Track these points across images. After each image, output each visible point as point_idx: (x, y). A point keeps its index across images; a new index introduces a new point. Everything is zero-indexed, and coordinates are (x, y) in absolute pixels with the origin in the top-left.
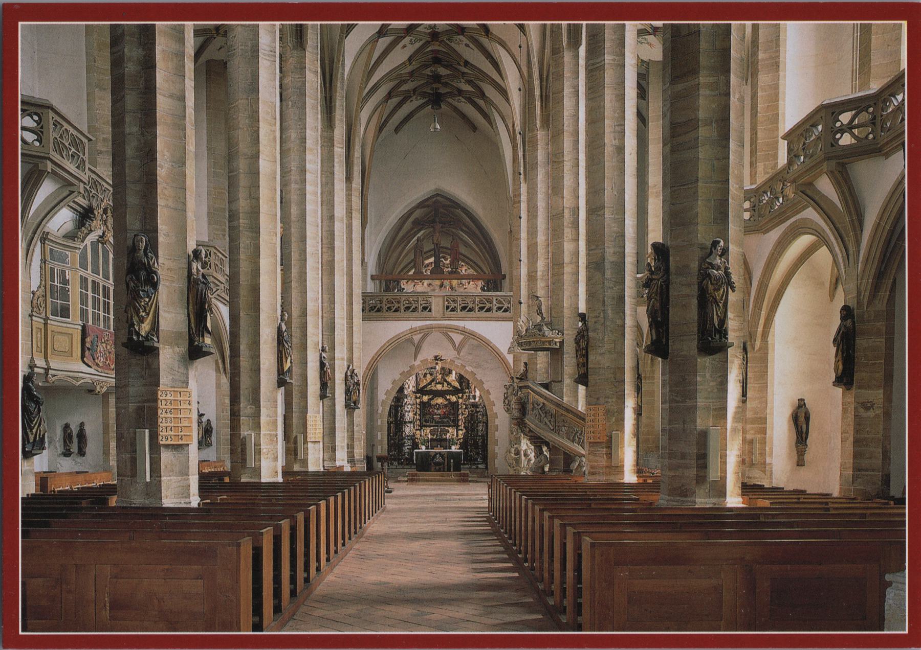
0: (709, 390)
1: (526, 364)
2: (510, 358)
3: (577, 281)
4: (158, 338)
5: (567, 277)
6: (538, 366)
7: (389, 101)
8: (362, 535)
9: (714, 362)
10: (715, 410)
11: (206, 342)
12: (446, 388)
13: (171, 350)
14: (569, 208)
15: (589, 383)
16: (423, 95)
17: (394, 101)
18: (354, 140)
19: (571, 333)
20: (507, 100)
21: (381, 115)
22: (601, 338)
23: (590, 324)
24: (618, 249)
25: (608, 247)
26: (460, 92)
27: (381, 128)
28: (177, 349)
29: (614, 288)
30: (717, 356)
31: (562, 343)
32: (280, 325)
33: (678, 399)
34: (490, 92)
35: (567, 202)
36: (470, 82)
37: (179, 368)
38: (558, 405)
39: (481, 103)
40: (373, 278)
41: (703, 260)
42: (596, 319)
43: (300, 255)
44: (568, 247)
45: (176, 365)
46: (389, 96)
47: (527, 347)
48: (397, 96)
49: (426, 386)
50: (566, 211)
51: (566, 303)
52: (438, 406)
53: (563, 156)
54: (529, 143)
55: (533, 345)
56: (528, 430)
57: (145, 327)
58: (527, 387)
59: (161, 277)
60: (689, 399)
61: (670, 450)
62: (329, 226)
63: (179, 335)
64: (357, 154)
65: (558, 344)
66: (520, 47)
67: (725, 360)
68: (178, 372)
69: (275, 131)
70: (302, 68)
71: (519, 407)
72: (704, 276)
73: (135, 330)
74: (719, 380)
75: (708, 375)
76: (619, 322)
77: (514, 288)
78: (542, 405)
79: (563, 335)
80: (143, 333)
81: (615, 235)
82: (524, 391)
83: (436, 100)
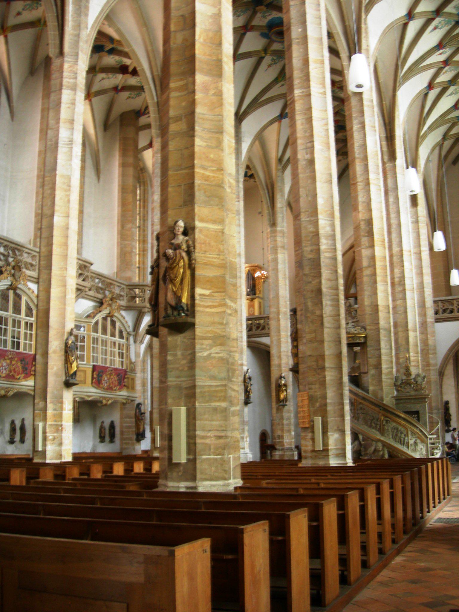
0: (180, 368)
9: (185, 340)
10: (186, 388)
14: (365, 220)
15: (300, 372)
19: (372, 327)
29: (313, 282)
30: (187, 334)
32: (67, 339)
50: (362, 223)
67: (193, 337)
74: (189, 357)
75: (179, 353)
76: (318, 313)
81: (311, 235)
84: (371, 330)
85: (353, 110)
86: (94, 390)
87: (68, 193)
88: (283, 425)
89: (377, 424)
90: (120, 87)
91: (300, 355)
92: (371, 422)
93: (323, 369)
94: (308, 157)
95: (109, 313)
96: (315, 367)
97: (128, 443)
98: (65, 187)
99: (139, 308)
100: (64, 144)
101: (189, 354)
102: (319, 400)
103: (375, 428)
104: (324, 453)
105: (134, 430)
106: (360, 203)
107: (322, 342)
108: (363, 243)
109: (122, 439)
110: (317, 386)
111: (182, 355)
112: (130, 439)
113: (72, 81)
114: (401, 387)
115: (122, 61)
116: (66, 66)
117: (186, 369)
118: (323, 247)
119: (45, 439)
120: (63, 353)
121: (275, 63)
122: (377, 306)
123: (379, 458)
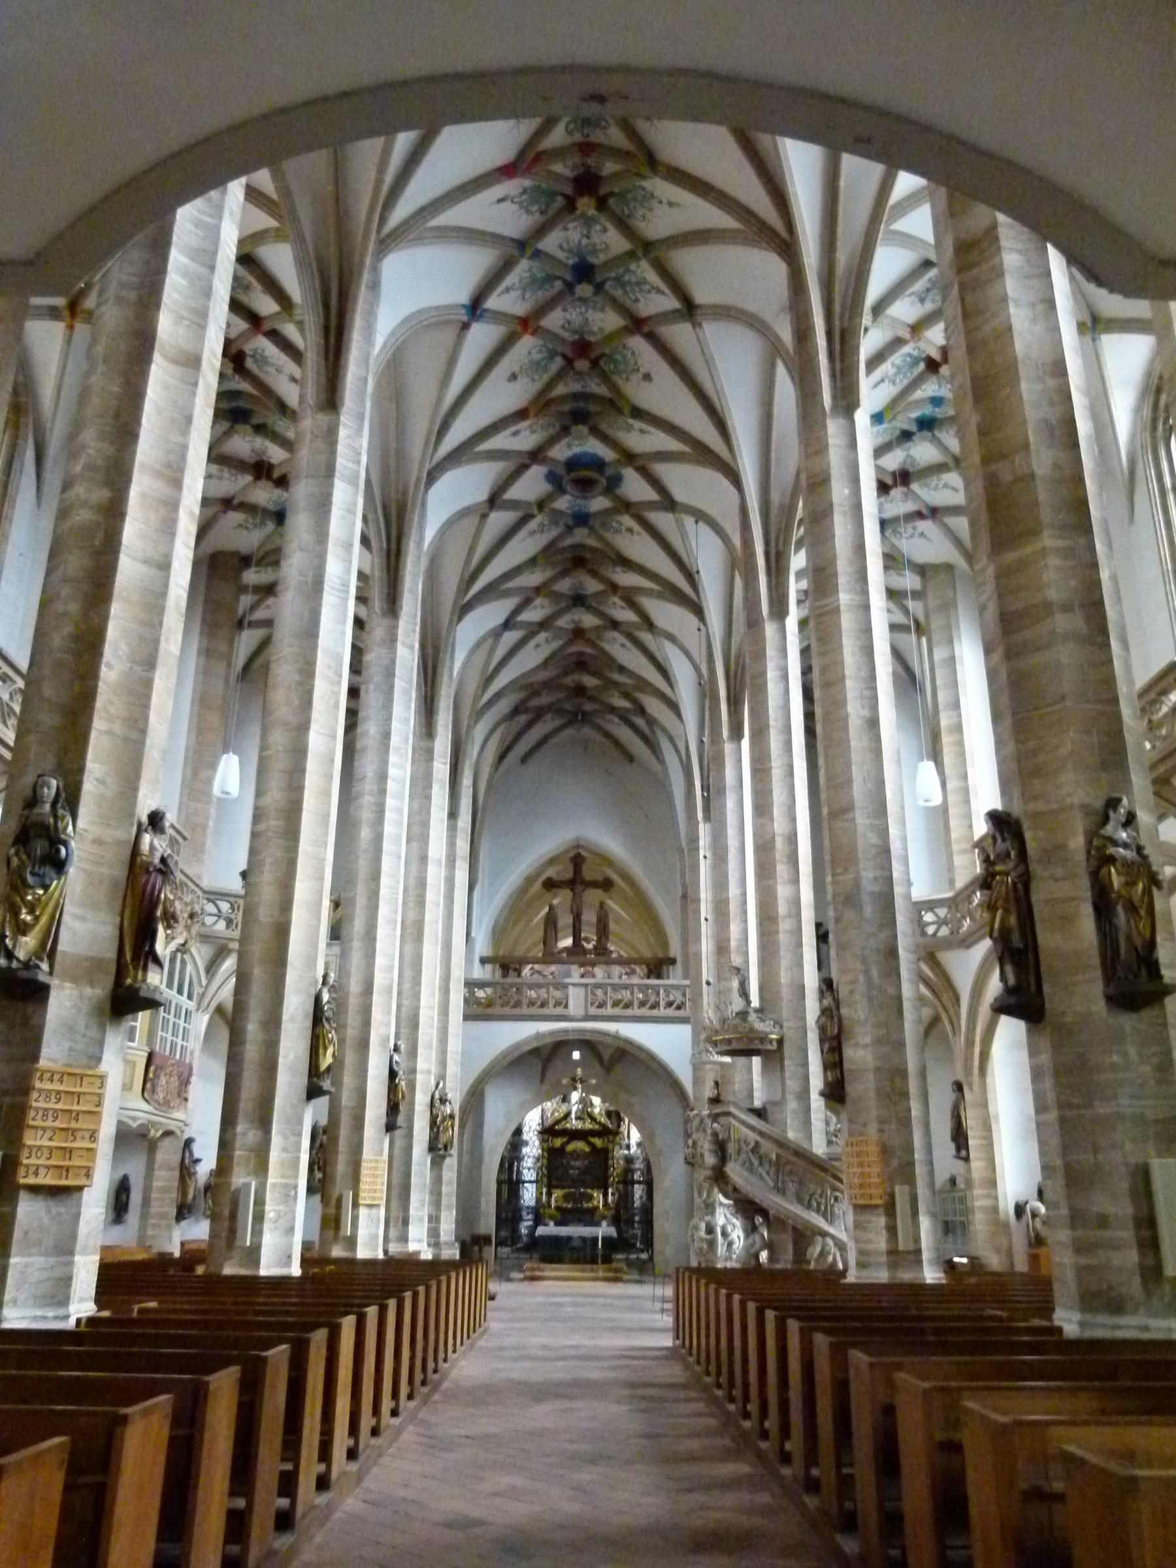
1: (717, 1084)
2: (685, 1076)
3: (800, 945)
4: (51, 967)
5: (783, 938)
6: (737, 1087)
7: (516, 719)
8: (436, 1386)
10: (1157, 1121)
11: (149, 980)
12: (589, 1125)
13: (75, 993)
15: (848, 1098)
16: (560, 712)
17: (523, 719)
18: (464, 762)
20: (678, 714)
21: (502, 740)
22: (862, 1017)
23: (843, 991)
24: (879, 873)
25: (865, 869)
26: (612, 709)
27: (502, 757)
28: (88, 991)
30: (1147, 1014)
31: (780, 1042)
33: (1076, 1101)
34: (654, 706)
35: (779, 825)
36: (626, 695)
37: (87, 1026)
38: (782, 1144)
39: (640, 722)
40: (484, 961)
41: (1092, 834)
42: (851, 987)
43: (370, 899)
44: (783, 892)
45: (81, 1027)
46: (516, 711)
47: (726, 1048)
48: (527, 711)
49: (558, 1122)
51: (784, 977)
52: (576, 1155)
53: (770, 761)
54: (713, 764)
55: (735, 1046)
56: (730, 1189)
57: (26, 945)
58: (729, 1114)
59: (76, 853)
60: (1101, 1101)
61: (1071, 1208)
62: (420, 872)
63: (96, 964)
64: (467, 781)
65: (775, 1044)
66: (699, 630)
68: (84, 1036)
69: (337, 694)
70: (392, 640)
71: (713, 1147)
72: (1100, 860)
73: (6, 947)
74: (1155, 1060)
75: (1132, 1052)
76: (891, 991)
77: (692, 972)
78: (752, 1144)
79: (781, 1027)
80: (21, 954)
81: (874, 851)
82: (723, 1120)
83: (578, 718)
84: (790, 1028)
85: (768, 644)
86: (144, 1106)
87: (336, 689)
88: (440, 1194)
89: (819, 1204)
90: (236, 502)
91: (846, 1066)
92: (809, 1202)
93: (905, 1095)
94: (865, 713)
95: (183, 945)
96: (888, 1089)
97: (159, 1226)
98: (330, 673)
99: (224, 941)
100: (332, 588)
101: (1155, 1054)
102: (898, 1153)
103: (818, 1211)
104: (912, 1257)
105: (174, 1195)
106: (775, 805)
107: (902, 1044)
108: (778, 873)
109: (144, 1216)
110: (893, 1127)
111: (1139, 1055)
112: (164, 1216)
113: (350, 465)
114: (836, 1136)
115: (264, 452)
116: (343, 433)
117: (1152, 1082)
118: (895, 875)
119: (259, 1218)
120: (309, 1023)
121: (542, 531)
122: (803, 986)
123: (825, 1266)
